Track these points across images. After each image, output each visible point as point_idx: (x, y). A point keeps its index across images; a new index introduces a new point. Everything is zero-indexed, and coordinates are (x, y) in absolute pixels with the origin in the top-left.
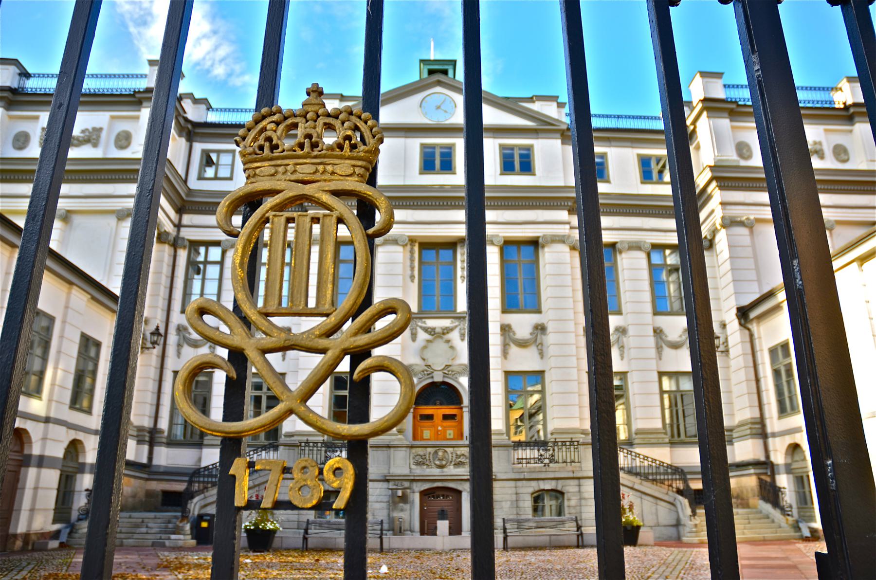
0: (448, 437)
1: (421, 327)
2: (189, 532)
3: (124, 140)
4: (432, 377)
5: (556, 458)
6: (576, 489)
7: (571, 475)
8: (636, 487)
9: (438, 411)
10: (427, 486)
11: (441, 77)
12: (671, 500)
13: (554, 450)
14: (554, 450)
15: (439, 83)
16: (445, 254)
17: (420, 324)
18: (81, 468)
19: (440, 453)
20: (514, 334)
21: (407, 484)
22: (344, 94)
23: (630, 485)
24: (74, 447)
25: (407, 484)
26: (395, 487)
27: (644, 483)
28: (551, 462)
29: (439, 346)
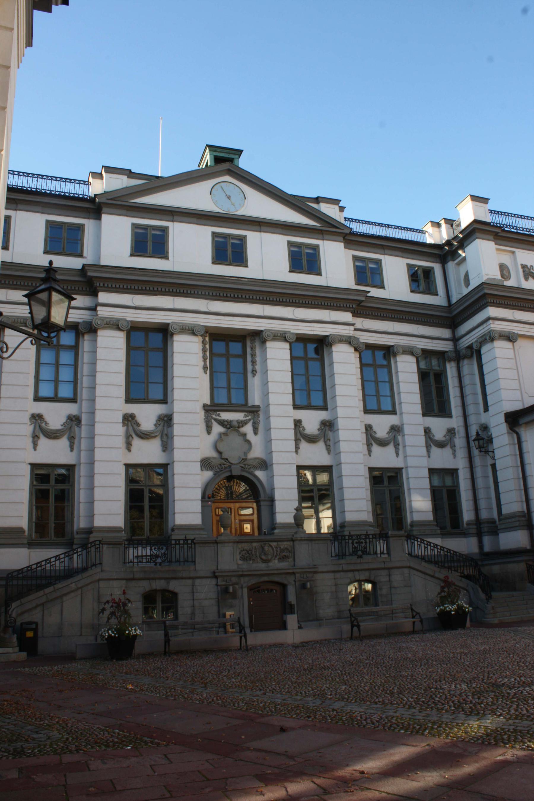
1: (216, 420)
2: (16, 644)
6: (387, 579)
7: (382, 565)
8: (437, 575)
10: (254, 581)
13: (366, 543)
16: (235, 348)
17: (214, 416)
20: (304, 429)
21: (234, 580)
22: (132, 171)
23: (432, 574)
25: (234, 580)
28: (363, 554)
29: (234, 440)
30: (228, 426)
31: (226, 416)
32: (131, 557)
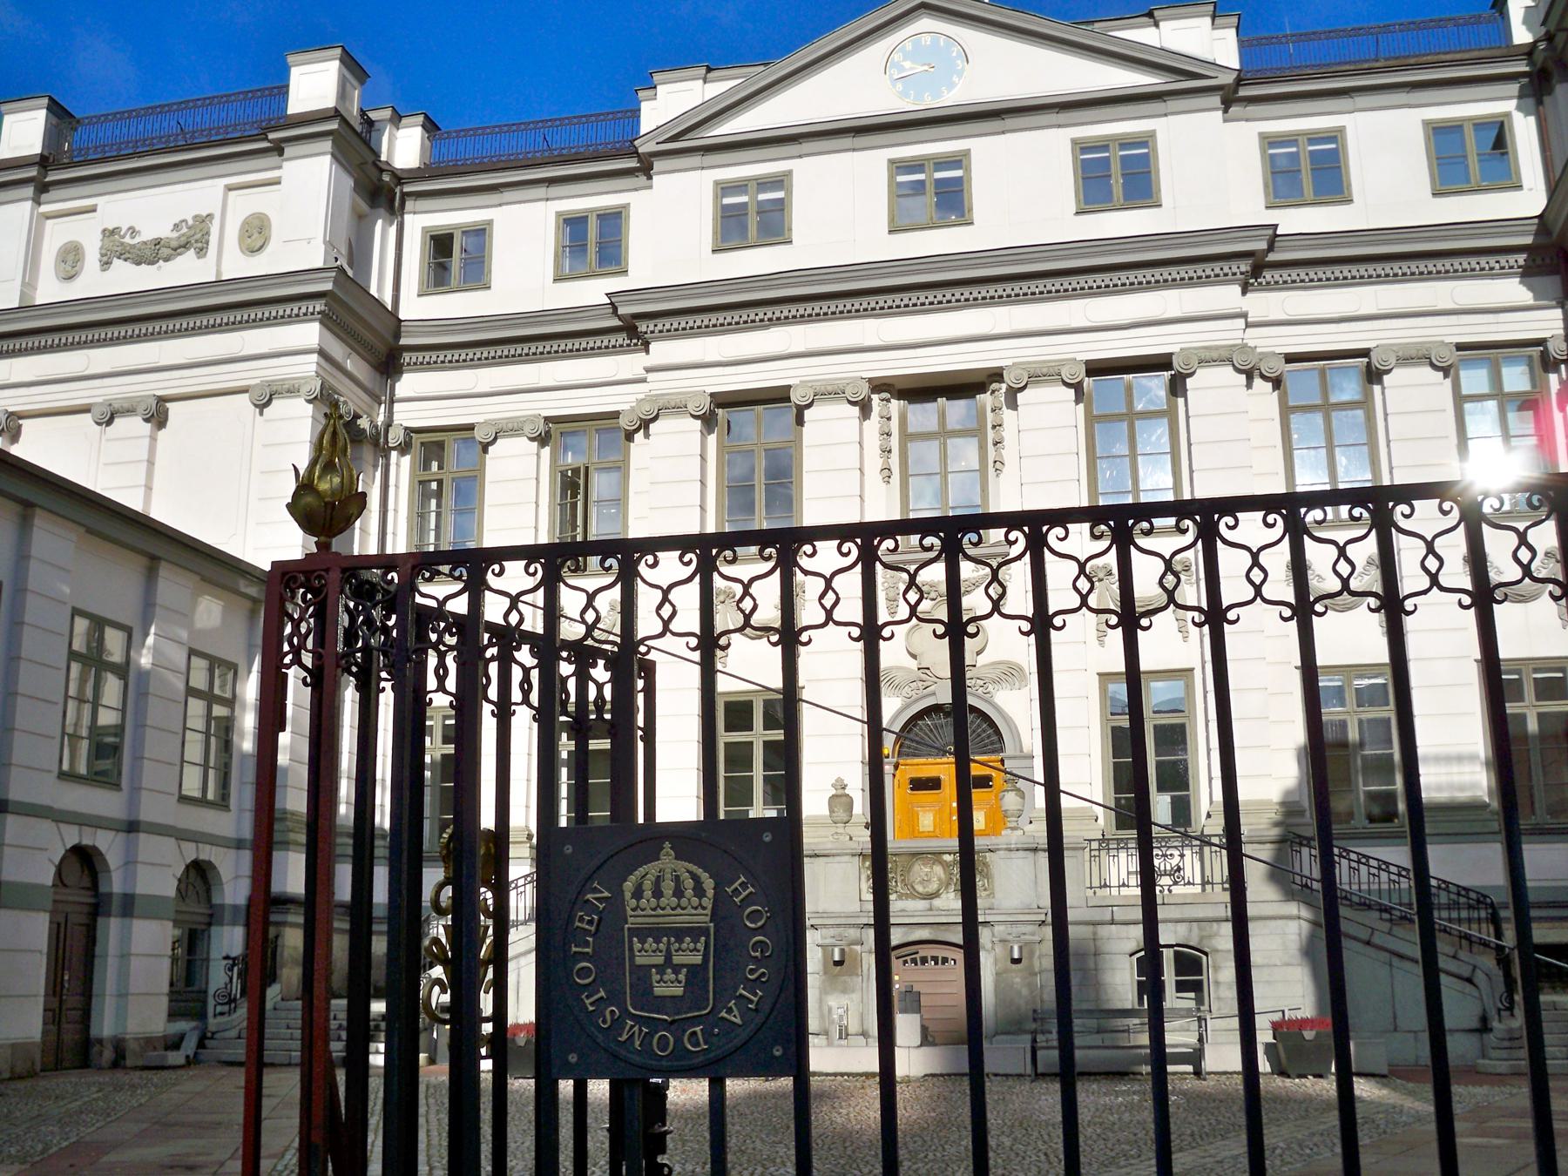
3: (256, 234)
5: (1188, 873)
8: (1377, 940)
12: (1466, 972)
13: (1182, 856)
14: (1182, 856)
18: (214, 916)
24: (200, 874)
27: (1397, 930)
28: (1176, 883)
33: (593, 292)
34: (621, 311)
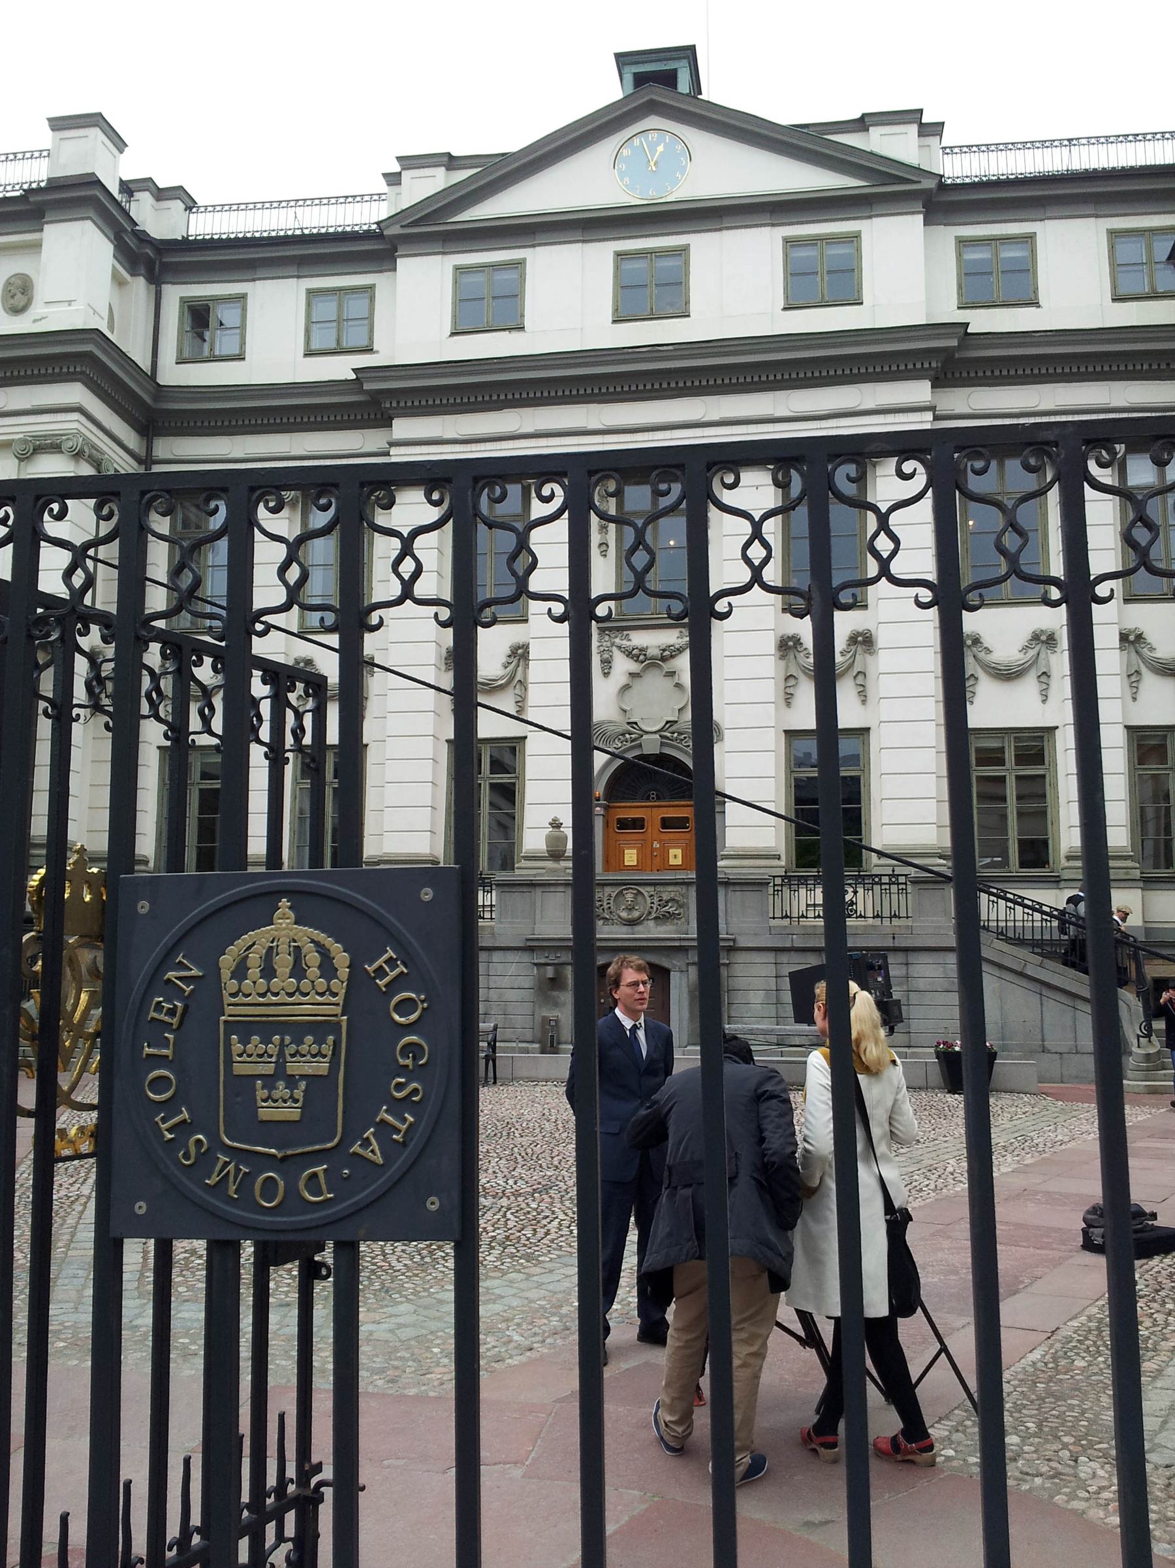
0: (672, 862)
1: (619, 647)
4: (640, 746)
5: (860, 908)
9: (653, 812)
11: (658, 93)
13: (855, 892)
14: (855, 892)
15: (652, 108)
17: (617, 641)
19: (629, 897)
22: (454, 154)
26: (543, 961)
27: (1049, 963)
29: (655, 683)
30: (642, 657)
31: (639, 639)
32: (803, 907)
33: (341, 368)
34: (366, 387)
